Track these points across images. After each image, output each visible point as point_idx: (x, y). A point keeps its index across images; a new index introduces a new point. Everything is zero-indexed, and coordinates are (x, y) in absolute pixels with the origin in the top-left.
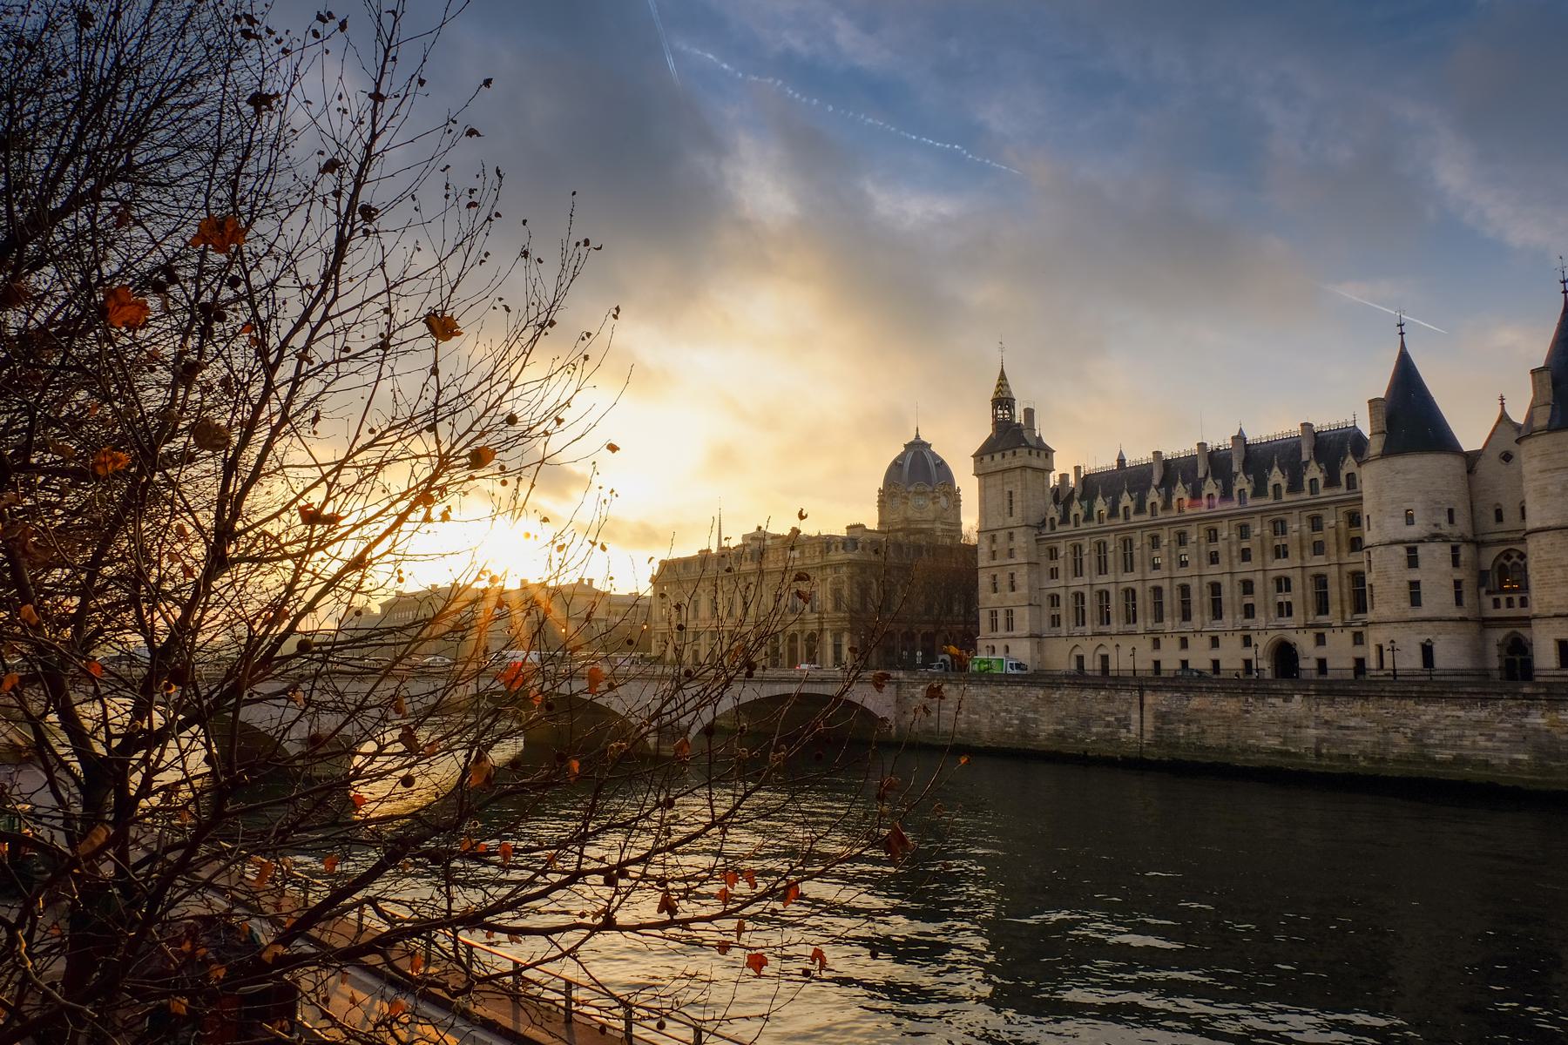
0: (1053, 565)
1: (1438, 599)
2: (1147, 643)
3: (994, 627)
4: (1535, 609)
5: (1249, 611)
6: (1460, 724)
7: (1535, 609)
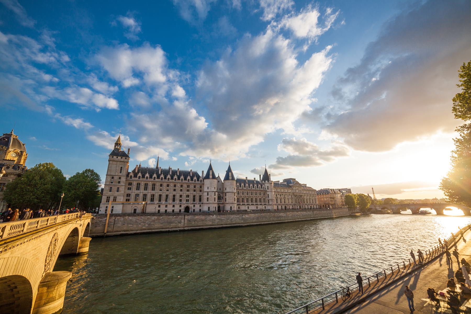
0: (130, 186)
2: (157, 206)
3: (108, 200)
4: (227, 202)
5: (181, 200)
6: (236, 218)
7: (227, 202)
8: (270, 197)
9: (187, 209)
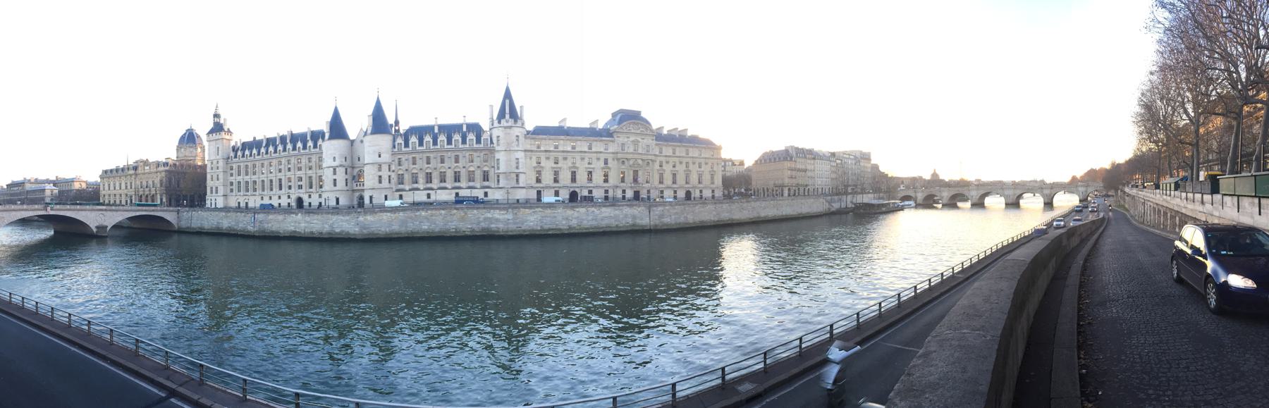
1: (341, 184)
8: (503, 169)
9: (300, 201)
